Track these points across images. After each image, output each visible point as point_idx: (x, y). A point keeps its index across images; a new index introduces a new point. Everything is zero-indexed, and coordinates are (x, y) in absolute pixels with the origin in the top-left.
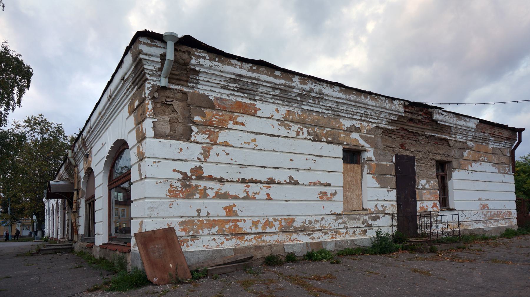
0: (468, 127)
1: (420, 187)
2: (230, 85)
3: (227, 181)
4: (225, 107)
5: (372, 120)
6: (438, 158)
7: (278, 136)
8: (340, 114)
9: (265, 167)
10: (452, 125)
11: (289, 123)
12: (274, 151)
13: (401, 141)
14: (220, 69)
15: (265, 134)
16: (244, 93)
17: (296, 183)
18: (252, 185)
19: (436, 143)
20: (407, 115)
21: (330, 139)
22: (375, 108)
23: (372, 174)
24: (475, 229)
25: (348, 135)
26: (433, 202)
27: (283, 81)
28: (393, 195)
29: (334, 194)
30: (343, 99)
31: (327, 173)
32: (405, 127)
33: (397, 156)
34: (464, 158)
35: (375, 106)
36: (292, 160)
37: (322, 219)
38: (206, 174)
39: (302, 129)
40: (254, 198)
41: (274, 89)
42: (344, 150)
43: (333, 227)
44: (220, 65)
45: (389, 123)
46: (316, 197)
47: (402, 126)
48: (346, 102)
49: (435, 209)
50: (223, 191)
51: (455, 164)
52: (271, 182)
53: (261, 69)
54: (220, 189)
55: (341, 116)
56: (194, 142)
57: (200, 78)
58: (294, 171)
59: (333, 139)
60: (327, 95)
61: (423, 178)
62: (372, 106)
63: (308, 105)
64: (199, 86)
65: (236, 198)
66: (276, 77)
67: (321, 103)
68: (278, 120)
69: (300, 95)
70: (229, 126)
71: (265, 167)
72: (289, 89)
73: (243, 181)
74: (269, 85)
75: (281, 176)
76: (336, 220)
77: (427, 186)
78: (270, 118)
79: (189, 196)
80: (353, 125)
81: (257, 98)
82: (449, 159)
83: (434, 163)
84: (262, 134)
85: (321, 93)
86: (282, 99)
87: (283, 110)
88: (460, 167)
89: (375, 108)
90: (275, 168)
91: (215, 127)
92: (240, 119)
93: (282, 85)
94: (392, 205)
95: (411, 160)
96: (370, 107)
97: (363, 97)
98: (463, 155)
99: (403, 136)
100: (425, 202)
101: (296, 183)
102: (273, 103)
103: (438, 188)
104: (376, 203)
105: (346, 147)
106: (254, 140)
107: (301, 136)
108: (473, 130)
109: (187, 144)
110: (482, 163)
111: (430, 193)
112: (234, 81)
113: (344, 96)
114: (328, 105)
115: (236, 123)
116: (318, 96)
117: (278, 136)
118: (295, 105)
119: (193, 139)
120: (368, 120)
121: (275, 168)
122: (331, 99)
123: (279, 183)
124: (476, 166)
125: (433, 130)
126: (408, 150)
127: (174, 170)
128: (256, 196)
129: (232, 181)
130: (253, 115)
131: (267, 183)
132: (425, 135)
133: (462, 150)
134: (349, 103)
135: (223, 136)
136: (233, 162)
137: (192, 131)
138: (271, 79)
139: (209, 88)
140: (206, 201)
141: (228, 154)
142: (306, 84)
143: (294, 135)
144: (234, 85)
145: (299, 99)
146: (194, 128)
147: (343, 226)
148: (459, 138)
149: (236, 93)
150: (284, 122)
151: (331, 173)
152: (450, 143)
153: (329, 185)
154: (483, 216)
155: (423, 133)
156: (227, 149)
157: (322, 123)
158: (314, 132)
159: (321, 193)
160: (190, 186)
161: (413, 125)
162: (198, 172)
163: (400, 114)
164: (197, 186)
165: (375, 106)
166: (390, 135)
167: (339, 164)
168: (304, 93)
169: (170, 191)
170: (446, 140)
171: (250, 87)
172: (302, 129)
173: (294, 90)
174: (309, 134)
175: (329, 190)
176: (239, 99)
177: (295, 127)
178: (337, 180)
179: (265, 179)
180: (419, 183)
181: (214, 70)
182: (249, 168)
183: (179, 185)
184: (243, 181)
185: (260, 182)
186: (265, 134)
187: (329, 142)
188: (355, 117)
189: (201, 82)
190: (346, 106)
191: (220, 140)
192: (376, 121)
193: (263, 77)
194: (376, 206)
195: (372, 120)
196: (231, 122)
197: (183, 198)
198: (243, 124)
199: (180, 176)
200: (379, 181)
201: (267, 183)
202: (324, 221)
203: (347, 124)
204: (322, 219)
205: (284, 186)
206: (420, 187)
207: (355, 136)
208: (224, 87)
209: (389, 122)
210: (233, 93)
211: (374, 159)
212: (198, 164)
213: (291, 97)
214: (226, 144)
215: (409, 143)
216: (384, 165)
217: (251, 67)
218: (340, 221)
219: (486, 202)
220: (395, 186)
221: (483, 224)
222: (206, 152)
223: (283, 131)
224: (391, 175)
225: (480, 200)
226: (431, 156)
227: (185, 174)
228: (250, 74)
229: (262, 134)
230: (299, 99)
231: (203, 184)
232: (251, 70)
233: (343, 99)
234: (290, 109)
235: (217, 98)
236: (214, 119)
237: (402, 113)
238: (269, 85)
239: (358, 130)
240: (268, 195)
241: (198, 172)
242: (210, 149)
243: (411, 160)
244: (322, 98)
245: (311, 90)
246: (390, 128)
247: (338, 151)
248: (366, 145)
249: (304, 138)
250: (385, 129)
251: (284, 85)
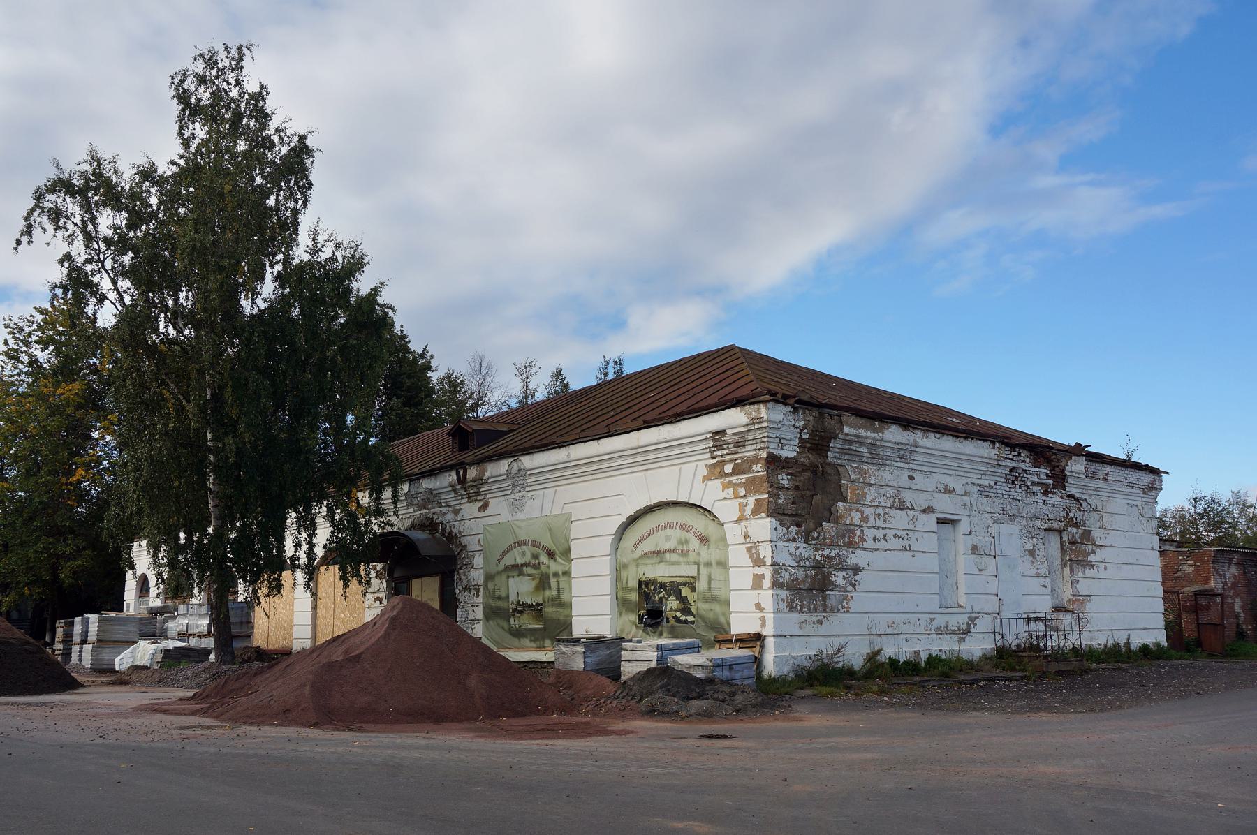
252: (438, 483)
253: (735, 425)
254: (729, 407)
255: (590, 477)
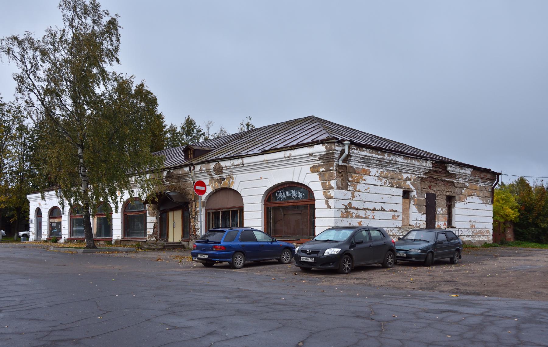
0: (466, 174)
1: (438, 213)
2: (361, 160)
3: (359, 209)
4: (359, 172)
5: (416, 173)
6: (448, 194)
7: (377, 185)
8: (402, 171)
9: (372, 202)
10: (457, 173)
11: (382, 178)
12: (376, 193)
13: (429, 184)
14: (359, 154)
15: (372, 185)
16: (365, 164)
17: (384, 210)
18: (367, 211)
19: (447, 184)
20: (433, 169)
21: (398, 186)
22: (418, 166)
23: (415, 205)
24: (466, 241)
25: (405, 183)
26: (444, 222)
27: (381, 157)
28: (424, 217)
29: (398, 216)
30: (405, 163)
31: (395, 204)
32: (432, 176)
33: (427, 193)
34: (463, 194)
35: (419, 165)
36: (382, 198)
37: (393, 230)
38: (352, 206)
39: (386, 181)
40: (368, 218)
41: (377, 160)
42: (403, 191)
43: (397, 235)
44: (359, 151)
45: (424, 174)
46: (391, 218)
47: (430, 175)
48: (405, 164)
49: (445, 226)
50: (358, 215)
51: (457, 198)
52: (374, 209)
53: (373, 151)
54: (357, 213)
55: (402, 172)
56: (349, 190)
57: (352, 159)
58: (383, 203)
59: (399, 185)
60: (398, 162)
61: (440, 207)
62: (417, 165)
63: (389, 167)
64: (351, 162)
65: (362, 218)
66: (379, 155)
67: (395, 166)
68: (377, 177)
69: (387, 163)
70: (360, 182)
71: (372, 202)
72: (383, 160)
73: (364, 209)
74: (376, 159)
75: (378, 207)
76: (399, 231)
77: (441, 212)
78: (374, 176)
79: (347, 217)
80: (408, 177)
81: (370, 166)
82: (454, 195)
83: (445, 197)
84: (371, 184)
85: (396, 161)
86: (379, 165)
87: (379, 171)
88: (460, 200)
89: (418, 166)
90: (376, 202)
91: (355, 182)
92: (364, 178)
93: (381, 158)
94: (424, 223)
95: (434, 196)
96: (416, 166)
97: (413, 161)
98: (462, 192)
99: (430, 181)
100: (440, 222)
101: (384, 210)
102: (376, 168)
103: (447, 213)
104: (416, 221)
105: (404, 189)
106: (369, 188)
107: (386, 185)
108: (469, 175)
109: (346, 191)
110: (473, 197)
111: (443, 217)
112: (363, 158)
113: (405, 161)
114: (398, 167)
115: (363, 180)
116: (394, 162)
117: (377, 185)
118: (384, 168)
119: (349, 189)
120: (414, 173)
121: (376, 202)
122: (400, 163)
123: (377, 210)
124: (469, 199)
125: (446, 177)
126: (432, 190)
127: (343, 204)
128: (369, 217)
129: (361, 209)
130: (369, 175)
131: (373, 210)
132: (441, 180)
133: (461, 189)
134: (407, 164)
135: (359, 187)
136: (361, 200)
137: (348, 185)
138: (377, 156)
139: (354, 163)
140: (352, 219)
141: (360, 196)
142: (390, 157)
143: (383, 184)
144: (363, 161)
145: (386, 164)
146: (349, 184)
147: (401, 234)
148: (461, 181)
149: (363, 164)
150: (380, 178)
151: (397, 205)
152: (455, 184)
153: (396, 211)
154: (472, 233)
155: (441, 179)
156: (360, 193)
157: (394, 177)
158: (391, 182)
159: (393, 215)
160: (348, 212)
161: (436, 174)
162: (350, 206)
163: (430, 169)
164: (350, 212)
165: (419, 165)
166: (424, 181)
167: (400, 200)
168: (389, 161)
169: (342, 214)
170: (453, 183)
171: (368, 161)
172: (386, 181)
173: (385, 161)
174: (389, 184)
175: (396, 214)
176: (364, 167)
177: (384, 180)
178: (400, 208)
179: (372, 208)
180: (437, 210)
181: (358, 154)
182: (367, 202)
183: (344, 211)
184: (364, 209)
185: (370, 210)
186: (372, 185)
187: (397, 187)
188: (409, 172)
189: (351, 160)
190: (405, 166)
191: (357, 189)
192: (418, 173)
193: (374, 155)
194: (416, 223)
195: (416, 173)
196: (361, 180)
197: (345, 218)
198: (365, 180)
199: (344, 207)
200: (418, 209)
201: (373, 210)
202: (394, 231)
203: (405, 176)
204: (393, 230)
205: (379, 212)
206: (438, 213)
207: (408, 183)
208: (359, 162)
209: (424, 173)
210: (362, 164)
211: (416, 196)
212: (350, 201)
213: (383, 164)
214: (359, 191)
215: (433, 185)
216: (420, 199)
217: (370, 151)
218: (400, 231)
219: (474, 223)
220: (425, 212)
221: (471, 238)
222: (353, 196)
223: (379, 183)
224: (424, 205)
225: (470, 221)
226: (444, 193)
227: (346, 206)
228: (369, 155)
229: (371, 184)
230: (386, 164)
231: (351, 211)
232: (370, 153)
233: (405, 163)
234: (382, 170)
235: (356, 168)
236: (355, 178)
237: (431, 168)
238: (376, 159)
239: (409, 179)
240: (373, 216)
241: (350, 206)
242: (354, 193)
243: (434, 196)
244: (396, 163)
245: (392, 160)
246: (424, 177)
247: (400, 192)
248: (413, 188)
249: (388, 186)
250: (422, 178)
251: (381, 158)
252: (181, 172)
253: (320, 151)
254: (318, 144)
255: (252, 171)
